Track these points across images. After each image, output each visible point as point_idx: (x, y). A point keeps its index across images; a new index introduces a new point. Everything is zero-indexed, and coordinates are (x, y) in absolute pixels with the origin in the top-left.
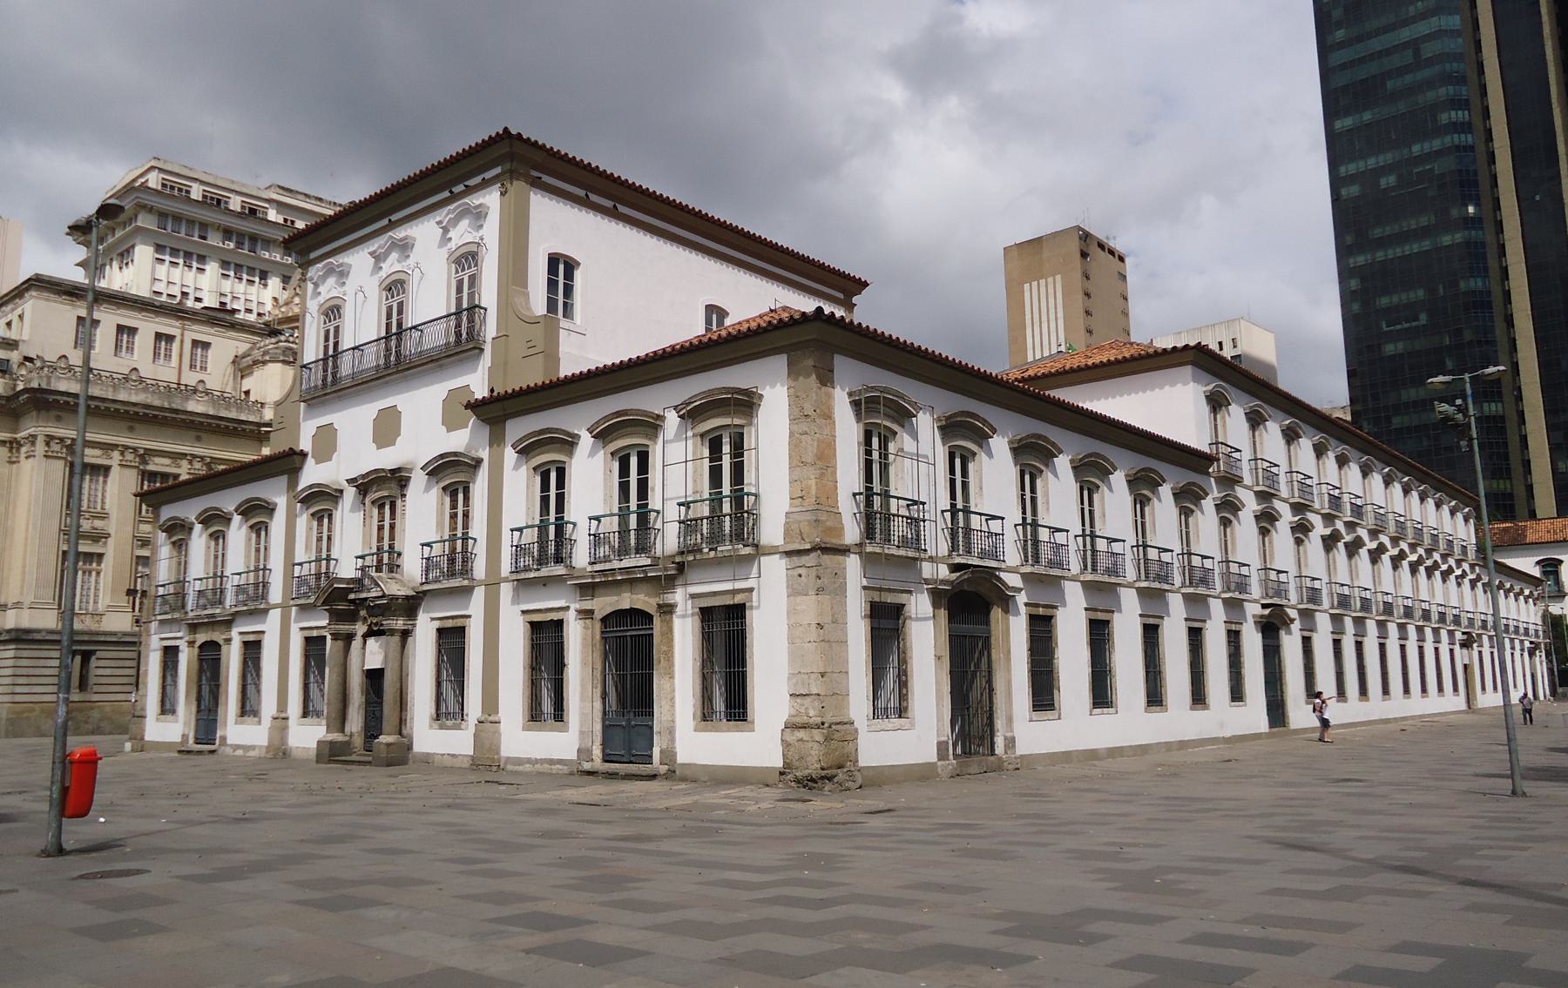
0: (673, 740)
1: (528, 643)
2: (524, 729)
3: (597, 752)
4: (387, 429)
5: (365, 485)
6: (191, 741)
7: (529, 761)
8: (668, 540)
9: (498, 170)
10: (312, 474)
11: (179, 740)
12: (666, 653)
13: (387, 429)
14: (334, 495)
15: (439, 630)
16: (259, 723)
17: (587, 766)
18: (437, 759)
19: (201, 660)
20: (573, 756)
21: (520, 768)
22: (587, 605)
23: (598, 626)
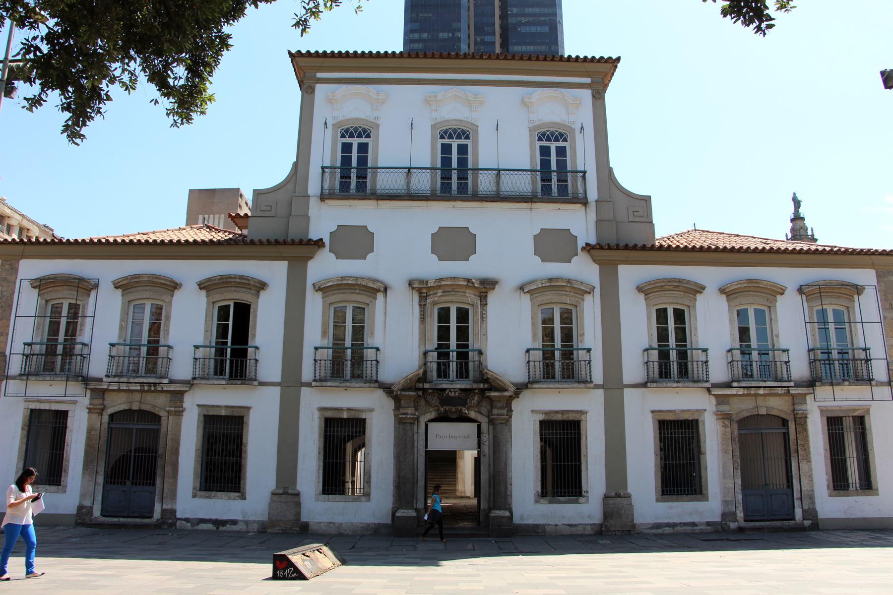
0: (813, 503)
1: (658, 436)
2: (657, 500)
3: (740, 514)
4: (454, 243)
5: (422, 289)
6: (97, 512)
7: (668, 525)
8: (799, 368)
9: (588, 80)
10: (324, 266)
11: (73, 511)
12: (803, 445)
13: (454, 243)
14: (375, 289)
15: (542, 423)
16: (243, 498)
17: (733, 525)
18: (548, 529)
19: (110, 430)
20: (717, 519)
21: (660, 531)
22: (725, 408)
23: (735, 426)
